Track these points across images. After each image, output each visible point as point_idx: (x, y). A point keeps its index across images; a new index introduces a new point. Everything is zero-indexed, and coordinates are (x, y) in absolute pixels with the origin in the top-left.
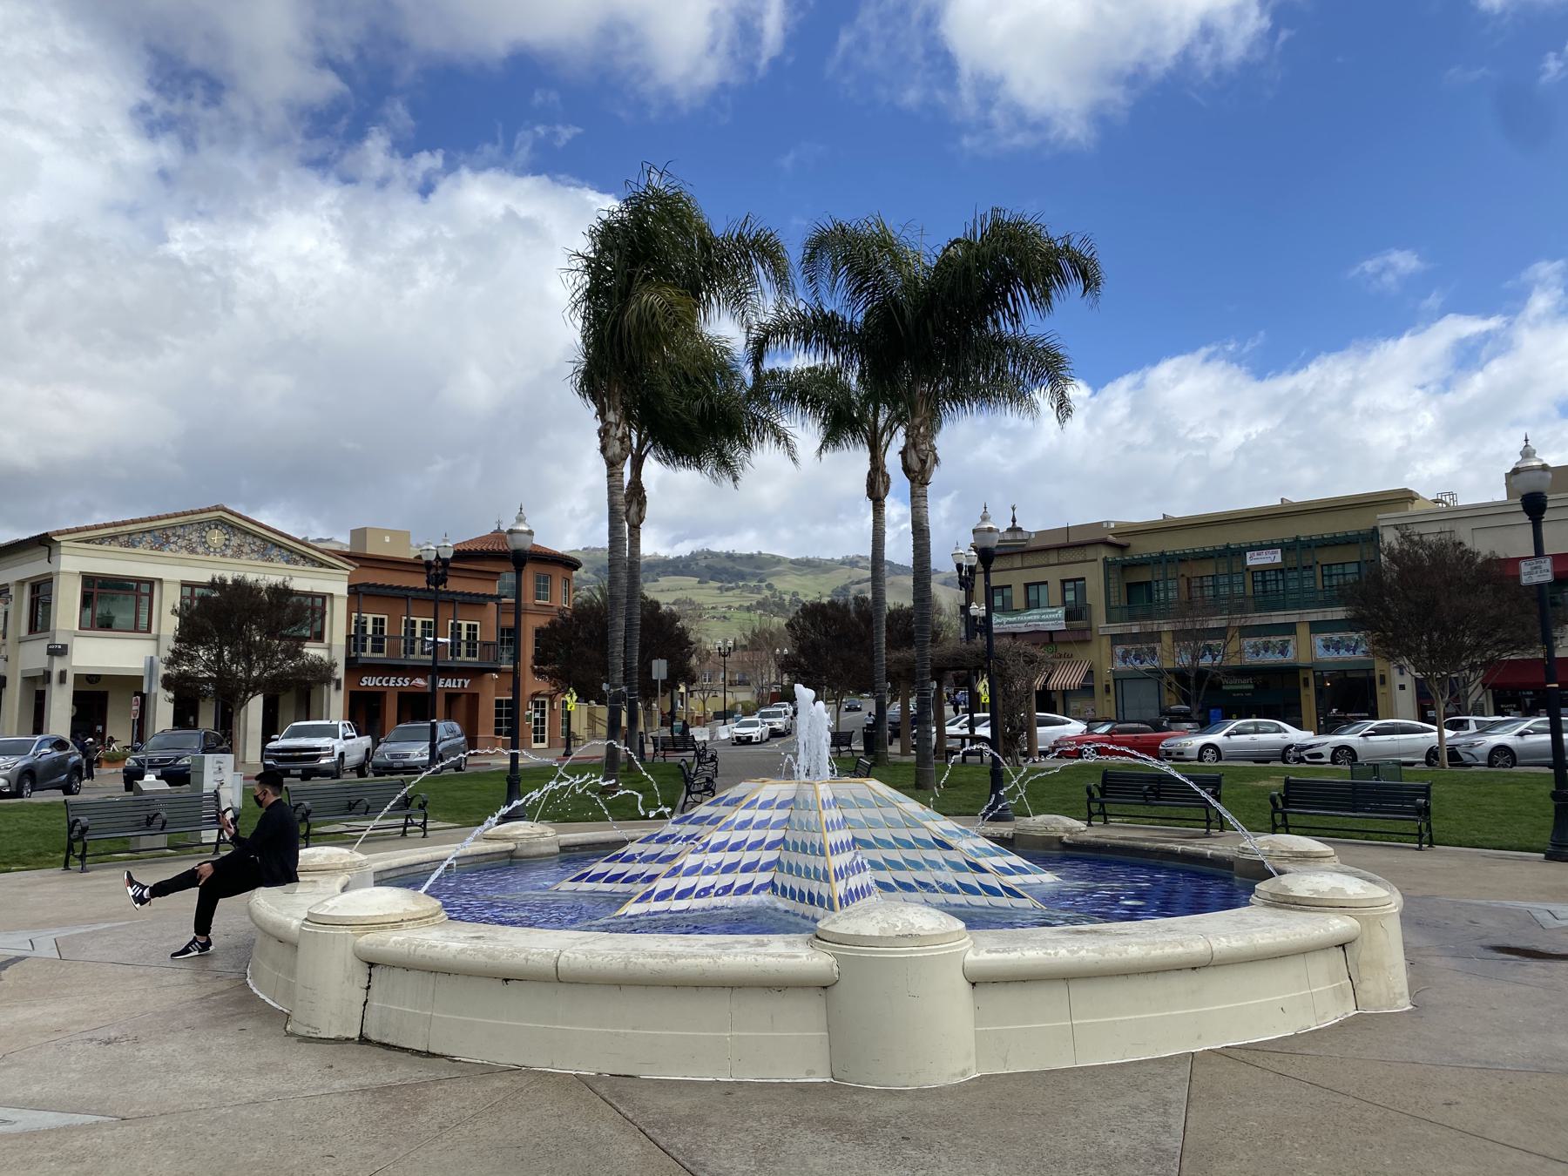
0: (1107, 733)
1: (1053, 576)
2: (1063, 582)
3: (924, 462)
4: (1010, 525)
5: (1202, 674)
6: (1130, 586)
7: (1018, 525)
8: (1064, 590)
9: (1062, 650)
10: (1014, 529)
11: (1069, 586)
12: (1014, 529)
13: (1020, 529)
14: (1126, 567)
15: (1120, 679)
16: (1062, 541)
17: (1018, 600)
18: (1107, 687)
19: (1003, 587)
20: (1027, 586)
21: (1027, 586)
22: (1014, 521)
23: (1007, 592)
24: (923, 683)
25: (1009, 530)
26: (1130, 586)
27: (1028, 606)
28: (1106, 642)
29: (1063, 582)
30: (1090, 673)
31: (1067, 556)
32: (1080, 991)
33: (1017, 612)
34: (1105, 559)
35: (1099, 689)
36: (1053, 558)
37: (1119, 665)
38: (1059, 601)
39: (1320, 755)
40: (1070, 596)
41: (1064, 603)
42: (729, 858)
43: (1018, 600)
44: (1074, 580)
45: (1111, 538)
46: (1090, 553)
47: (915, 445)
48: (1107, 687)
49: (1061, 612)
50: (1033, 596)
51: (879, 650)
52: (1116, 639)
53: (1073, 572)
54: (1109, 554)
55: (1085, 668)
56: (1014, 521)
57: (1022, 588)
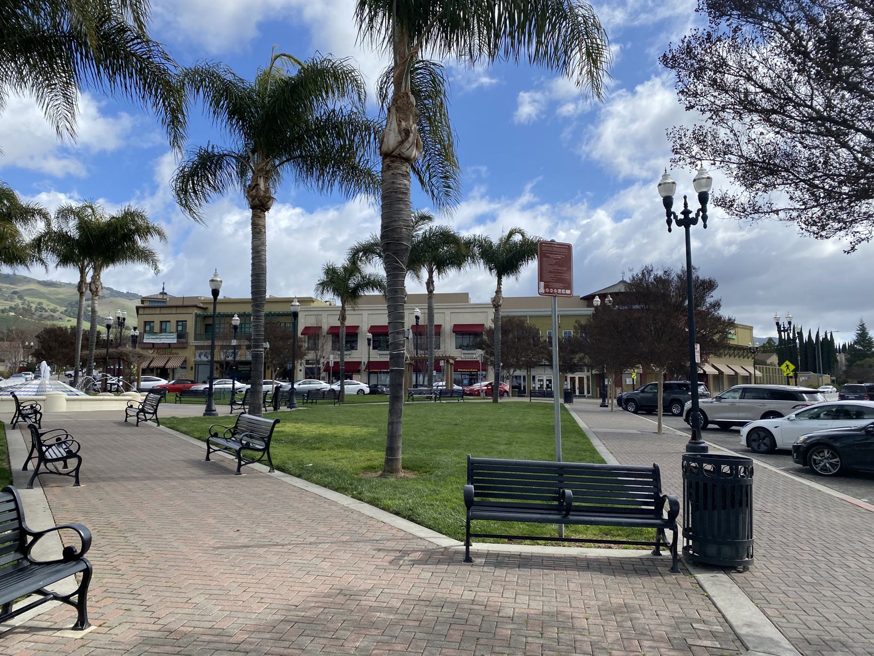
0: (173, 384)
1: (173, 319)
2: (178, 322)
3: (97, 288)
4: (162, 291)
5: (228, 363)
6: (207, 325)
7: (165, 291)
8: (178, 325)
9: (174, 351)
10: (163, 293)
11: (180, 323)
12: (163, 293)
13: (166, 294)
14: (205, 317)
15: (197, 364)
16: (181, 304)
17: (157, 328)
18: (192, 367)
19: (151, 322)
20: (161, 322)
21: (161, 322)
22: (163, 289)
23: (152, 324)
24: (90, 363)
25: (161, 293)
26: (207, 325)
27: (161, 331)
28: (194, 348)
29: (178, 322)
30: (185, 361)
31: (179, 311)
32: (83, 402)
33: (156, 333)
34: (196, 313)
35: (189, 367)
36: (174, 311)
37: (198, 358)
38: (174, 330)
39: (242, 391)
40: (180, 328)
41: (177, 330)
42: (26, 393)
43: (157, 328)
44: (182, 321)
45: (201, 305)
46: (190, 310)
47: (94, 282)
48: (192, 367)
49: (175, 335)
50: (164, 327)
51: (78, 350)
52: (197, 348)
53: (181, 318)
54: (198, 312)
55: (183, 359)
56: (163, 289)
57: (159, 323)
